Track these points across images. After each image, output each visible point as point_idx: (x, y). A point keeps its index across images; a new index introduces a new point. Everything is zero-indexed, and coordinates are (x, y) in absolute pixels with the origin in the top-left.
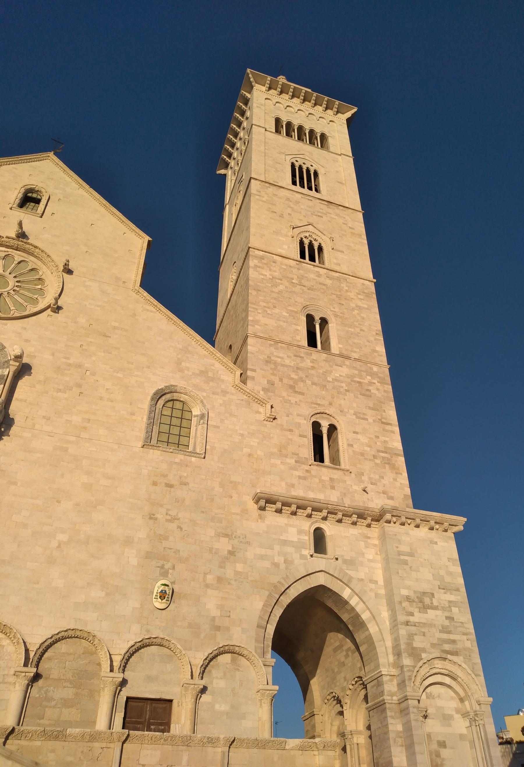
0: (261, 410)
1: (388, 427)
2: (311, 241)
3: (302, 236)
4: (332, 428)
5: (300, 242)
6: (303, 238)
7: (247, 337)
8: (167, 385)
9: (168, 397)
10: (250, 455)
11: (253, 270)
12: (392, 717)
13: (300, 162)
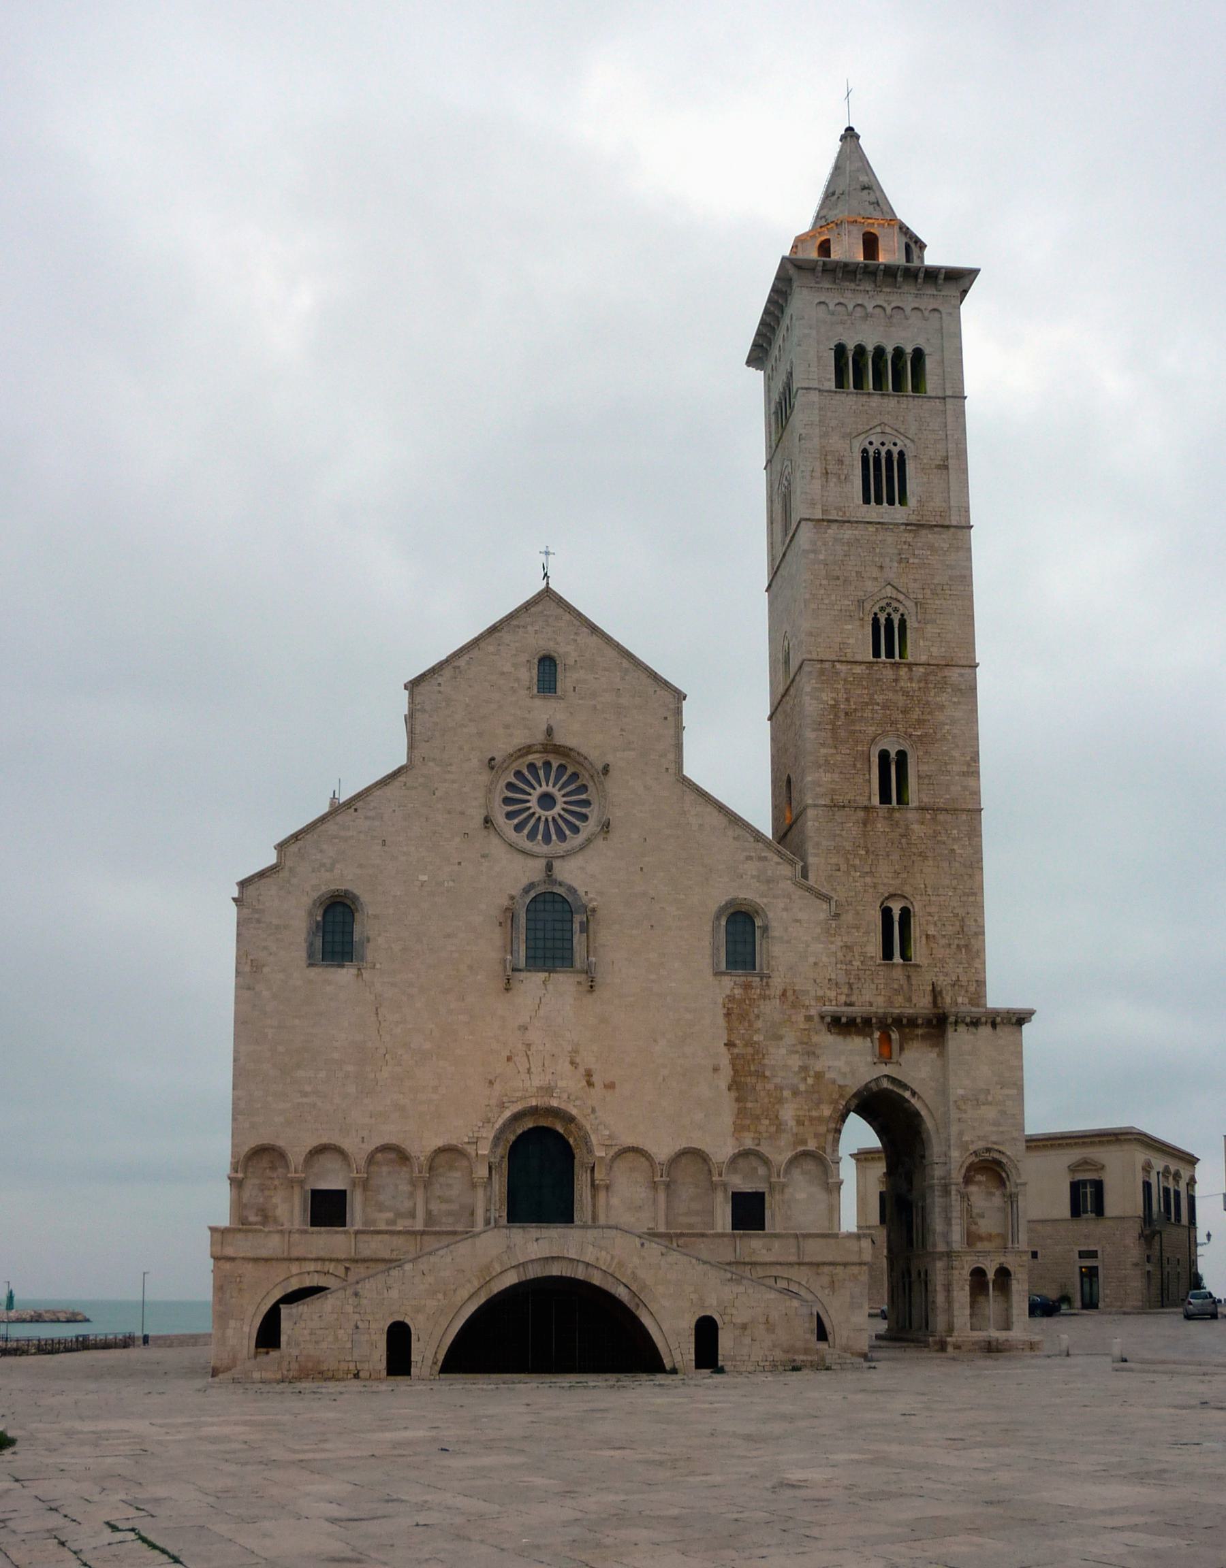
0: (825, 906)
1: (972, 899)
2: (889, 614)
3: (876, 609)
4: (906, 914)
5: (873, 624)
6: (878, 611)
7: (805, 809)
8: (727, 898)
9: (732, 910)
10: (815, 964)
11: (809, 698)
12: (939, 1196)
13: (877, 444)
